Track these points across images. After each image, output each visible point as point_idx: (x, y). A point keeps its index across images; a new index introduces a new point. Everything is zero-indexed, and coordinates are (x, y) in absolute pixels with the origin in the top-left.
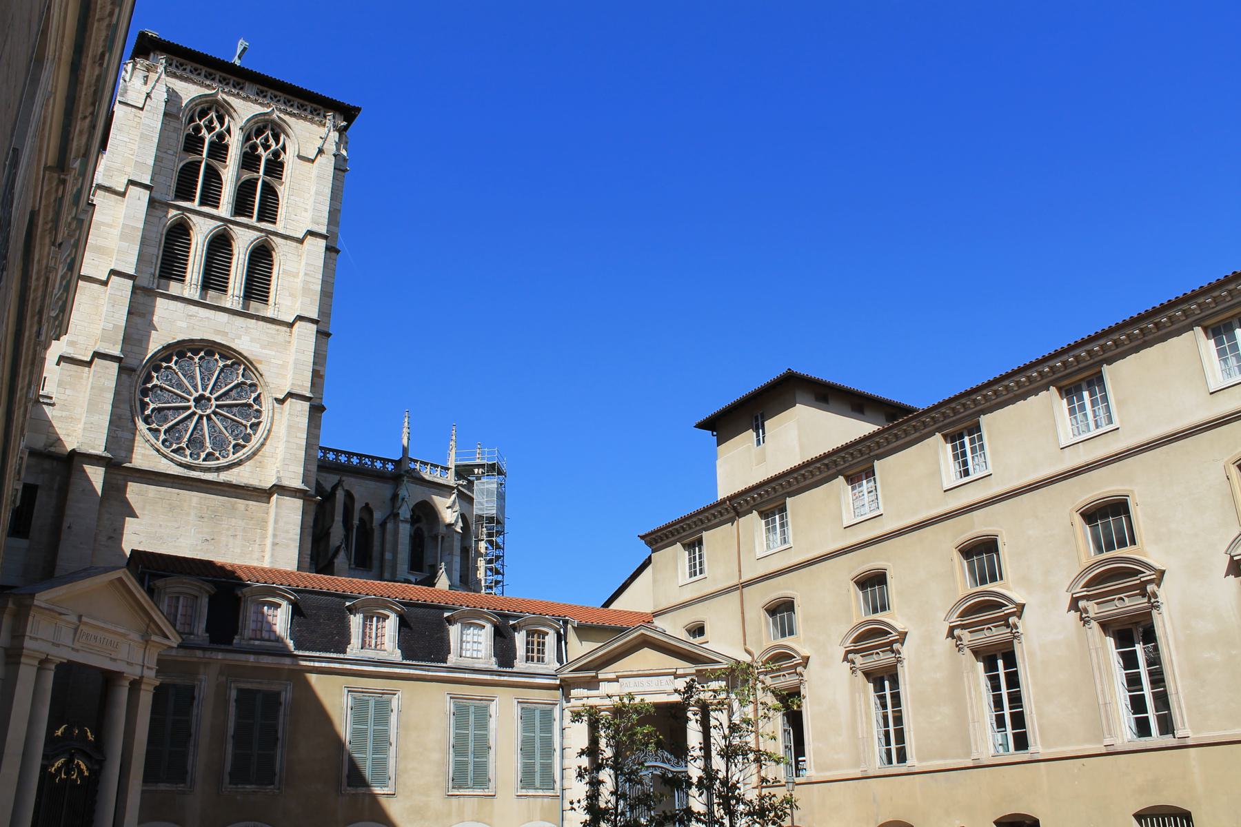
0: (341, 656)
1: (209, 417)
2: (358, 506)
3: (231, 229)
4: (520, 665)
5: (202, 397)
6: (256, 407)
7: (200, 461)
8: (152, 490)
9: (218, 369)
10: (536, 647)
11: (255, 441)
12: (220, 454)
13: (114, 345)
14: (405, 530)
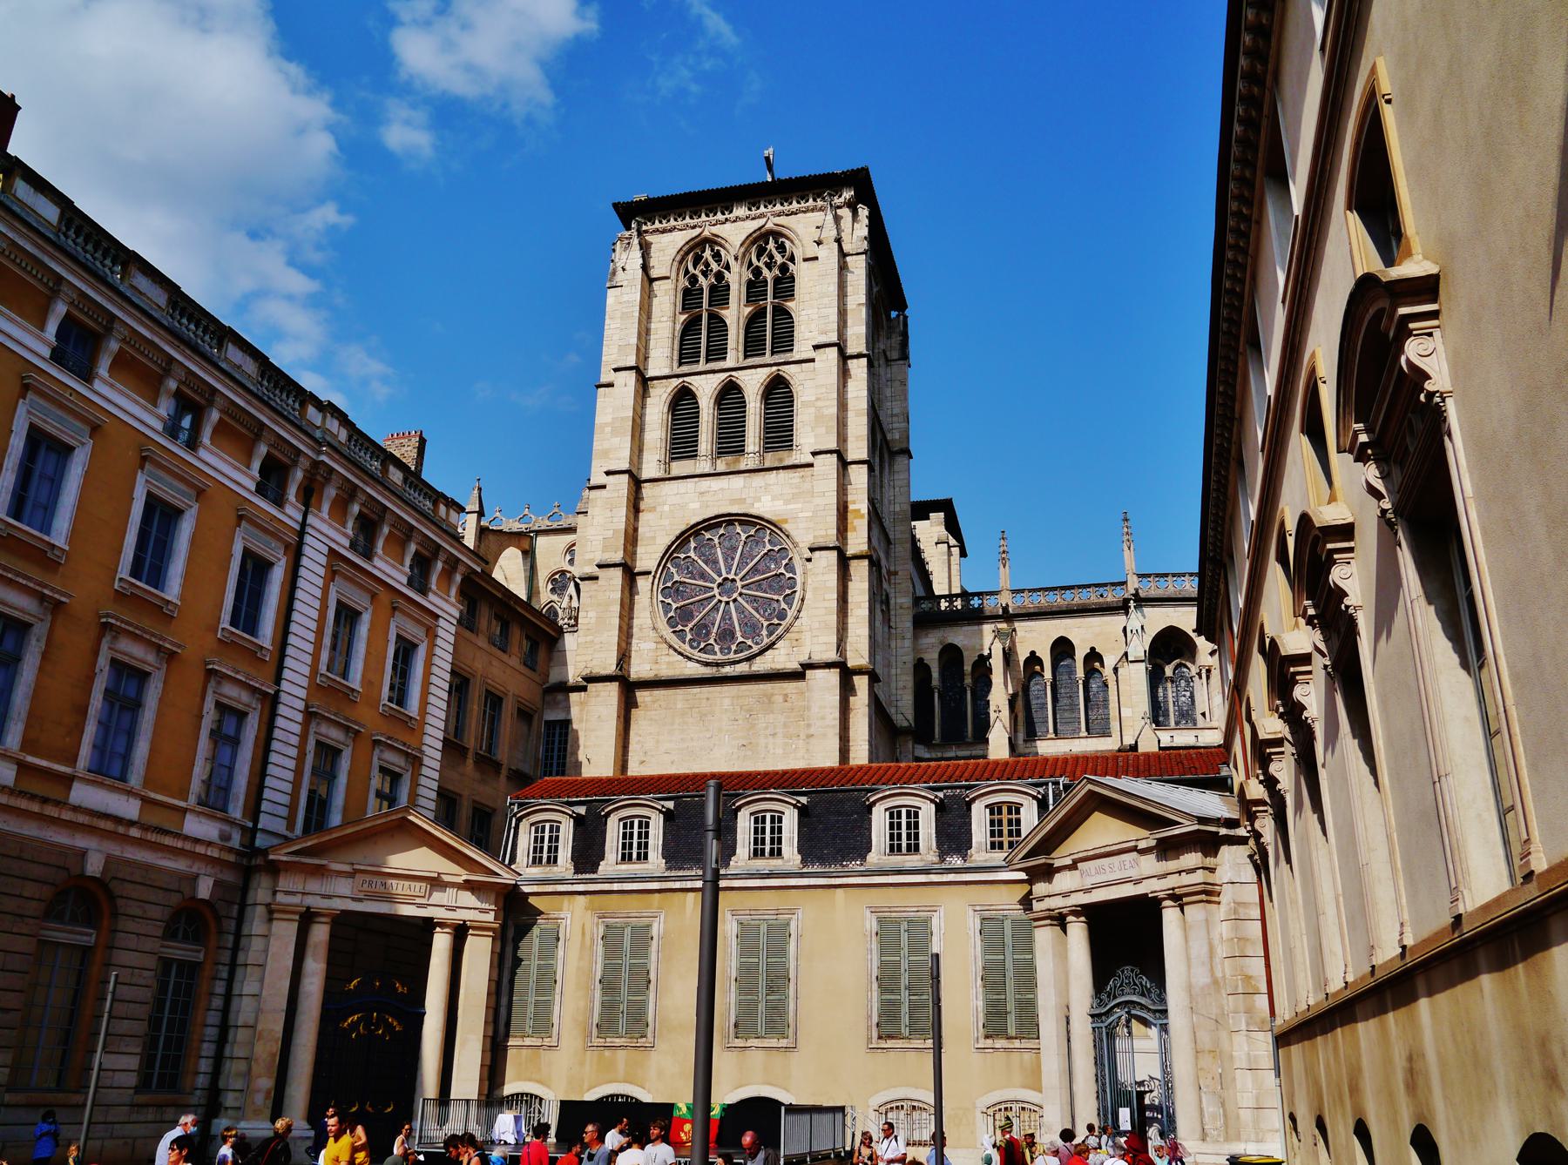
2: (1080, 654)
6: (788, 575)
7: (732, 656)
9: (742, 543)
10: (1005, 829)
11: (791, 614)
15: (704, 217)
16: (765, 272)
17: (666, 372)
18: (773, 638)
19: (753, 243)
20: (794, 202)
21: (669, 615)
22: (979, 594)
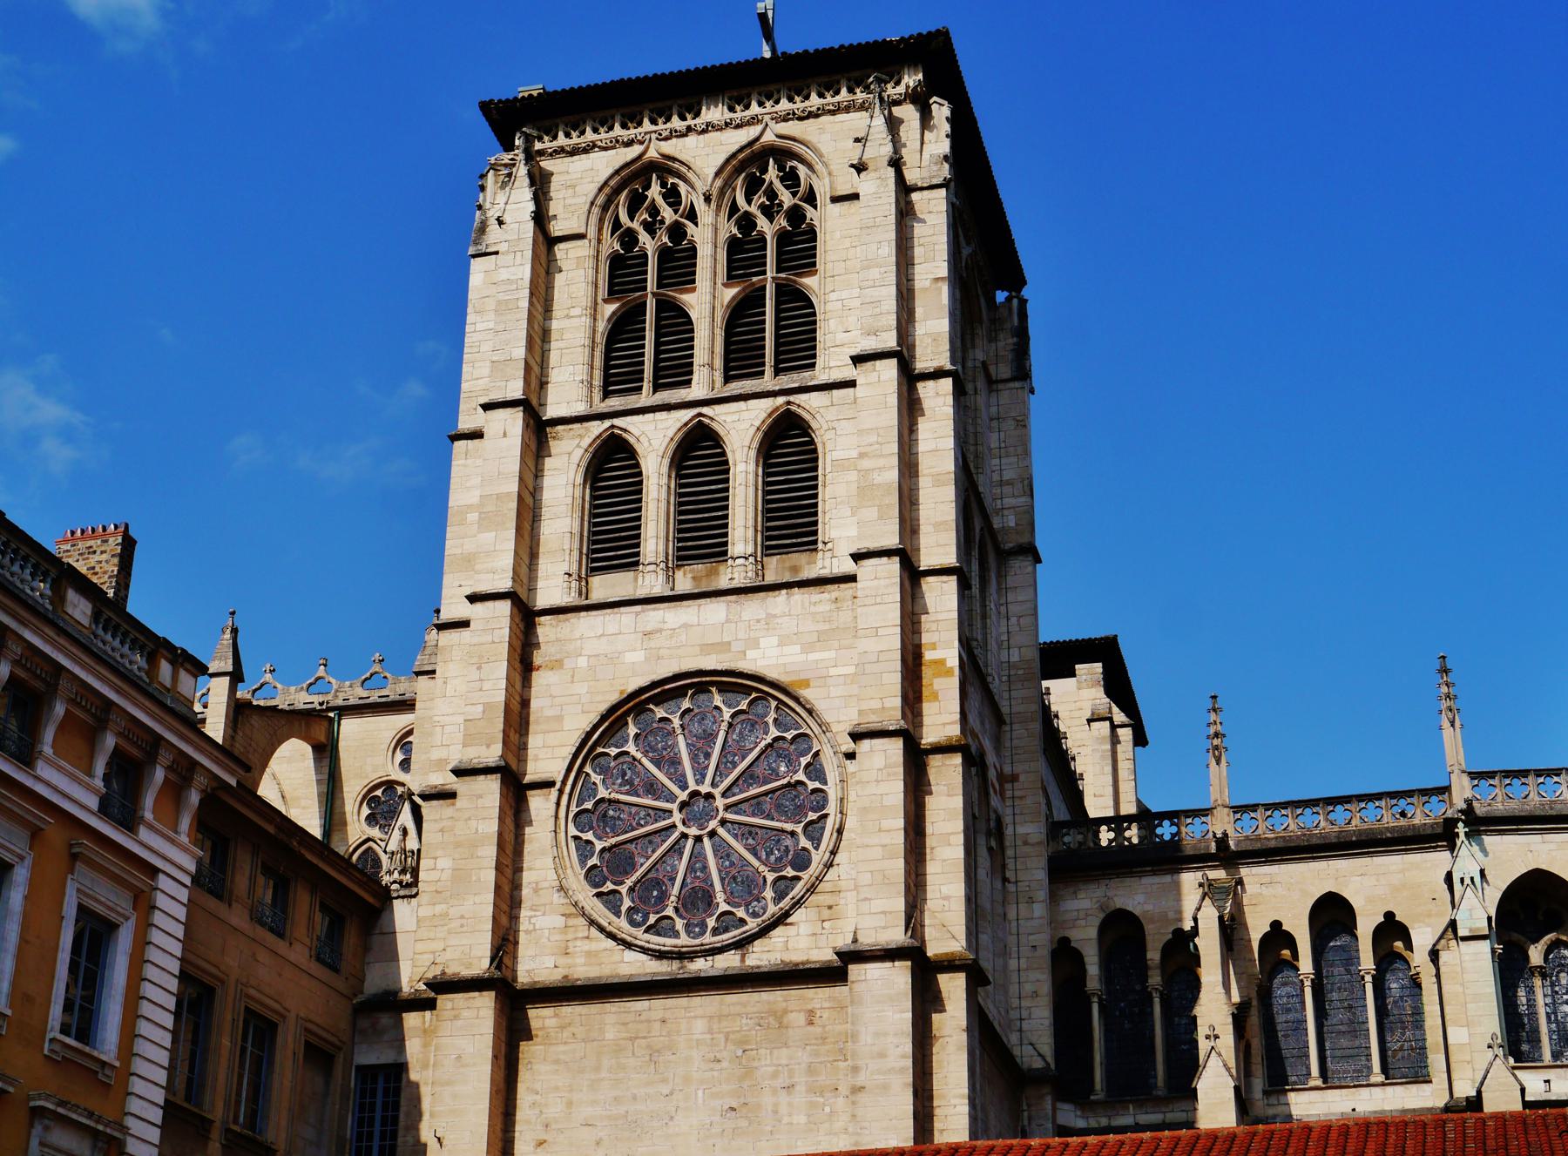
2: (1366, 927)
3: (712, 419)
6: (812, 785)
7: (708, 939)
9: (724, 726)
11: (818, 857)
12: (747, 912)
15: (647, 125)
16: (762, 223)
17: (580, 408)
18: (786, 903)
19: (738, 171)
20: (814, 96)
21: (590, 863)
22: (1173, 816)
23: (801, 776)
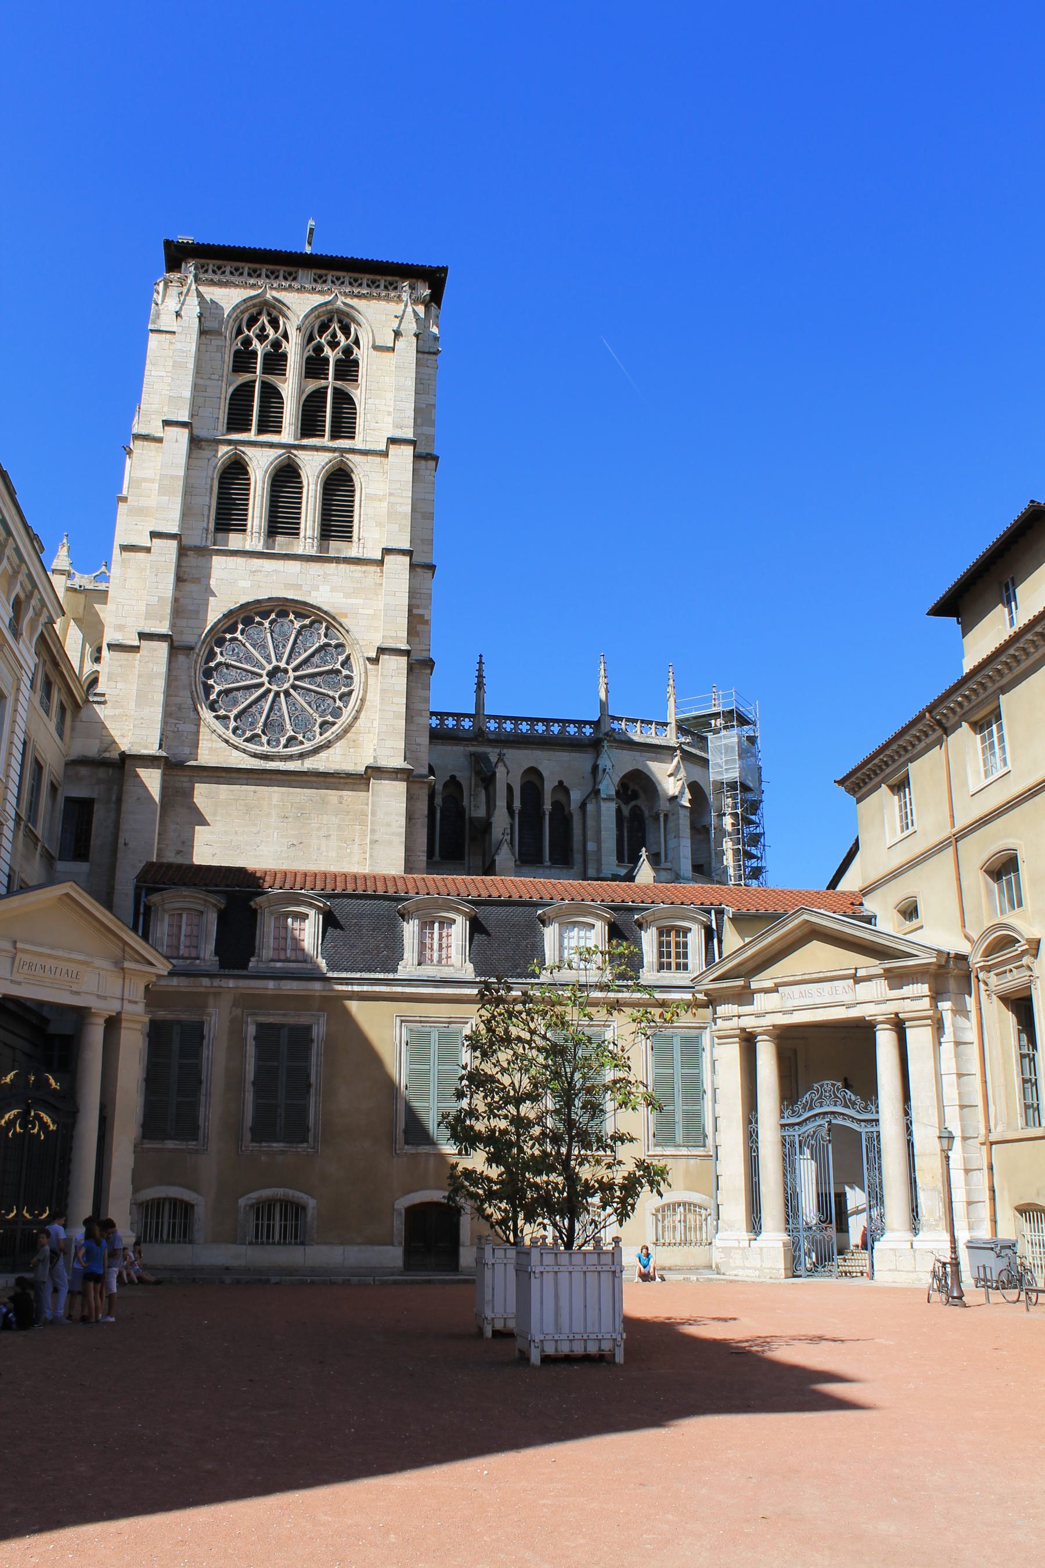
0: (391, 976)
1: (287, 694)
2: (549, 786)
3: (296, 456)
4: (649, 975)
5: (277, 669)
6: (345, 672)
7: (280, 749)
8: (224, 791)
9: (294, 632)
10: (673, 950)
12: (304, 737)
13: (161, 622)
14: (608, 811)
16: (327, 351)
23: (338, 666)
